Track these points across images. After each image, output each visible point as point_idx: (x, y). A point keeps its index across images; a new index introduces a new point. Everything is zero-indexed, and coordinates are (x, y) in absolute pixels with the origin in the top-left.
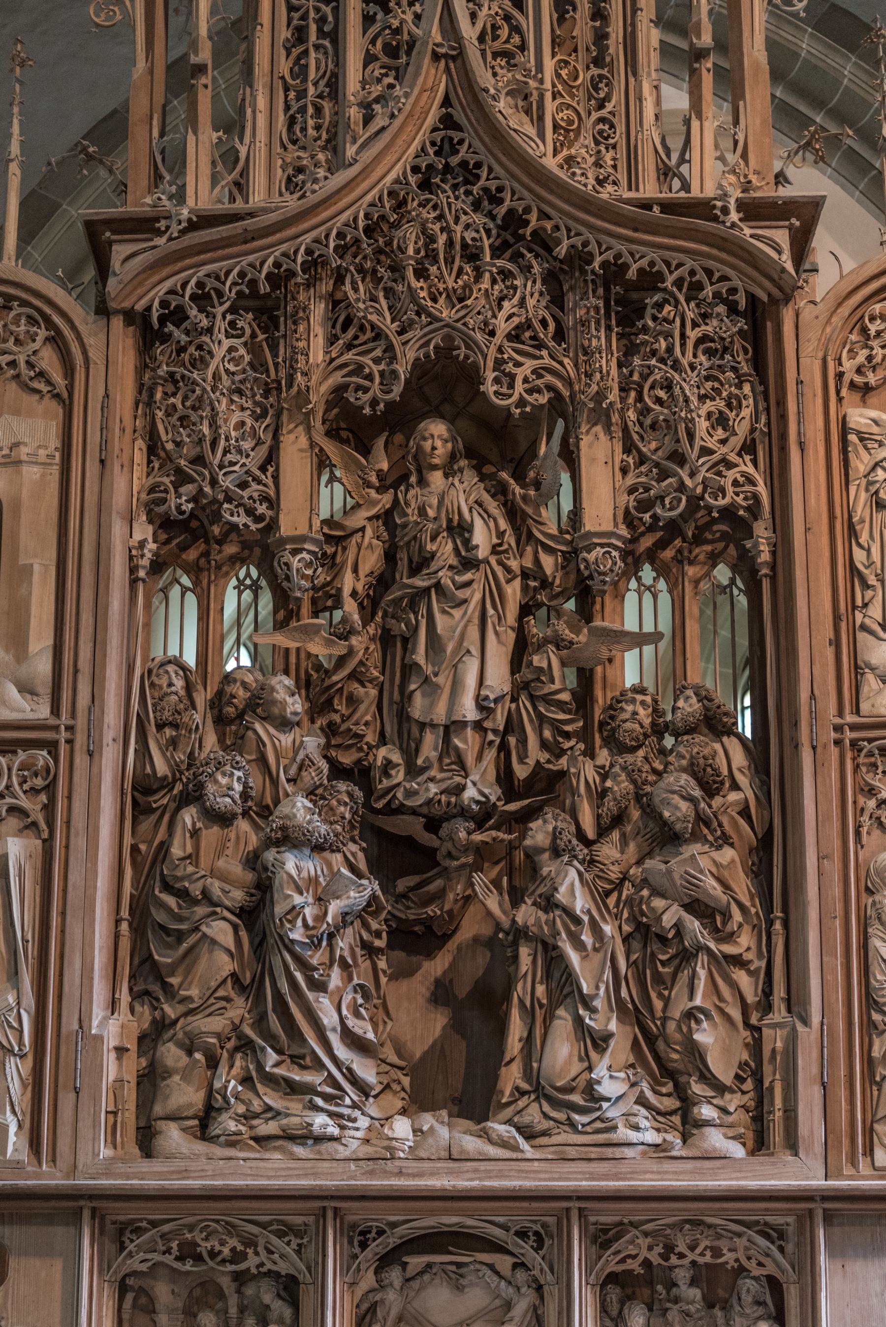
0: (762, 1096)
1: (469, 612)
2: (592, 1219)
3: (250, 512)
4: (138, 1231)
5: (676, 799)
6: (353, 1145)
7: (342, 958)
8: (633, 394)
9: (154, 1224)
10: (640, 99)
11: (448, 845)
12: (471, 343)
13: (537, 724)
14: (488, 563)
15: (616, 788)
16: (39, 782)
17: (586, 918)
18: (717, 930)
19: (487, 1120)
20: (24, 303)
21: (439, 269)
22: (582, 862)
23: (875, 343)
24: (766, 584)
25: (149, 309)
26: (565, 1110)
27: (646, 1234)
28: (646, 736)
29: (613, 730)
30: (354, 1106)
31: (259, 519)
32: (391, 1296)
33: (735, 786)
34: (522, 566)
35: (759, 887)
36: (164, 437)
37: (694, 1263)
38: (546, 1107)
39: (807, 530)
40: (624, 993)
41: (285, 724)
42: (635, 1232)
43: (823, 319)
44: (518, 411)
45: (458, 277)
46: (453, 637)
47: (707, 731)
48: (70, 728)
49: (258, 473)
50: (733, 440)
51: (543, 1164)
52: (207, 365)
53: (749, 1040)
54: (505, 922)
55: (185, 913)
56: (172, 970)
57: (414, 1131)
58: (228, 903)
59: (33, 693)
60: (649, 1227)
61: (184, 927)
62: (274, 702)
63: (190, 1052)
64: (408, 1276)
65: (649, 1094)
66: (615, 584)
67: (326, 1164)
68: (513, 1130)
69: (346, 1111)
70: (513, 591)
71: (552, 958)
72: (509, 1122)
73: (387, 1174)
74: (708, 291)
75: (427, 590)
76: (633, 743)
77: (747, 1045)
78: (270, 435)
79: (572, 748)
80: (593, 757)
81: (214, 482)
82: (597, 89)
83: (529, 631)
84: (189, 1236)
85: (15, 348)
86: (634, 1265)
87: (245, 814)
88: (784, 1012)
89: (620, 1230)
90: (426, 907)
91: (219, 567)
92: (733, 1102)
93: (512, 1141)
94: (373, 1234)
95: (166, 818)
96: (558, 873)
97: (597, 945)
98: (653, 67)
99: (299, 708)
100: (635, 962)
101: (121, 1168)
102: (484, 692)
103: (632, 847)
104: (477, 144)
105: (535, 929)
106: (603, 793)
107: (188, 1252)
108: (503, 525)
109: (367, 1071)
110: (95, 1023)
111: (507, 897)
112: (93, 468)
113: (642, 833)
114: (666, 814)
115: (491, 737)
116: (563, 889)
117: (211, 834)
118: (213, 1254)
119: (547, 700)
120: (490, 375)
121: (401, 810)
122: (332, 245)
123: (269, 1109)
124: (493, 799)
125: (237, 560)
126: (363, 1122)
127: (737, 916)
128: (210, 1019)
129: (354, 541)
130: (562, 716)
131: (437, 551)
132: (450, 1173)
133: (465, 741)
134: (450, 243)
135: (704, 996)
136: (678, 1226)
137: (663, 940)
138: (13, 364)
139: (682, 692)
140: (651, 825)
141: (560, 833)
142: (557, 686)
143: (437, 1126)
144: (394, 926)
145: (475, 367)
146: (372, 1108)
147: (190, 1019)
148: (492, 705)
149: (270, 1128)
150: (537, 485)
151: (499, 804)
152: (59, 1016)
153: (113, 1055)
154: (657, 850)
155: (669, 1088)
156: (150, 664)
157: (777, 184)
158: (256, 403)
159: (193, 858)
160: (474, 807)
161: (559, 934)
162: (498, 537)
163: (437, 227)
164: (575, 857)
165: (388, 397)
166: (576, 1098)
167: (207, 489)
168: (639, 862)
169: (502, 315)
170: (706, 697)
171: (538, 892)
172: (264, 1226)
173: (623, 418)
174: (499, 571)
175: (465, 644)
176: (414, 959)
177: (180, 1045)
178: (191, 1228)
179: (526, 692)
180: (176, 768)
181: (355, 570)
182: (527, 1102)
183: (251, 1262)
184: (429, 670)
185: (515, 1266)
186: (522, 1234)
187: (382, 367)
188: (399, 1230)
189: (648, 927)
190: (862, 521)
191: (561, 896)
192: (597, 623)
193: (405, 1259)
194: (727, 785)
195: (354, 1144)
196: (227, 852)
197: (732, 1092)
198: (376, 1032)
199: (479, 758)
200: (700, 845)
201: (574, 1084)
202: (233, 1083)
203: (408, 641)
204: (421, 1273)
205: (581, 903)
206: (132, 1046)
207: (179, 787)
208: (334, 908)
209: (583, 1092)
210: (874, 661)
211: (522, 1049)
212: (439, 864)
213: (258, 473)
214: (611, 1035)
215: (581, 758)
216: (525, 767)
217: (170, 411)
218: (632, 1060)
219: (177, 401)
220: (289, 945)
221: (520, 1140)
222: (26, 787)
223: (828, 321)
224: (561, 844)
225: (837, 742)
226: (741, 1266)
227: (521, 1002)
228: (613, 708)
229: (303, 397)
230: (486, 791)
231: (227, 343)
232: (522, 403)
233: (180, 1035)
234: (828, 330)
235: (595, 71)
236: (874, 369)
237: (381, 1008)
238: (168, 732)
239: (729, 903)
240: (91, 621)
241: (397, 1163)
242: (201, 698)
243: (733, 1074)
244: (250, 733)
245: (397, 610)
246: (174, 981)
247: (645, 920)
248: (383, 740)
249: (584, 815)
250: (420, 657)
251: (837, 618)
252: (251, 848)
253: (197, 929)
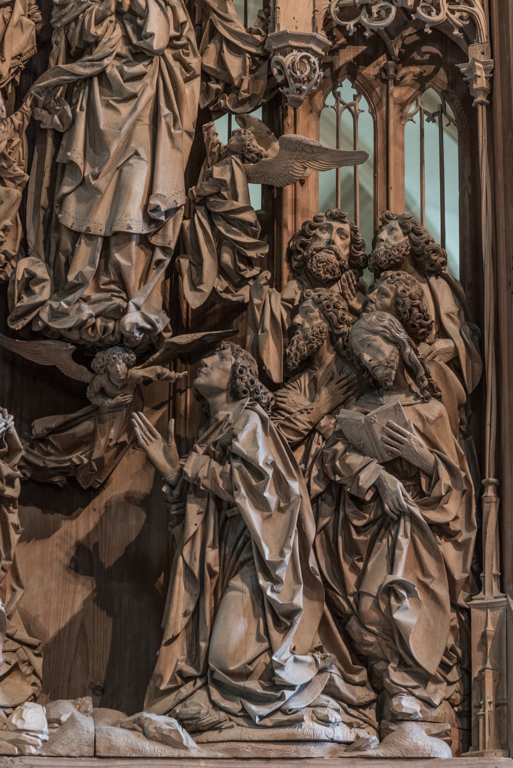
1: (140, 108)
11: (101, 380)
13: (215, 245)
14: (164, 56)
15: (307, 325)
17: (270, 472)
19: (140, 709)
22: (266, 407)
26: (239, 699)
28: (343, 269)
29: (305, 260)
33: (443, 334)
34: (202, 64)
35: (468, 448)
38: (216, 695)
40: (312, 562)
46: (119, 135)
47: (412, 269)
66: (311, 95)
68: (175, 722)
71: (226, 518)
76: (329, 276)
79: (254, 278)
80: (280, 289)
83: (209, 139)
90: (70, 454)
93: (173, 736)
96: (237, 418)
97: (282, 505)
100: (324, 528)
103: (324, 394)
105: (207, 483)
106: (294, 328)
108: (183, 16)
111: (173, 444)
113: (337, 378)
115: (159, 255)
116: (243, 436)
124: (160, 327)
130: (245, 239)
131: (103, 36)
133: (129, 258)
139: (384, 223)
140: (347, 370)
141: (241, 372)
142: (240, 203)
144: (29, 475)
148: (163, 218)
151: (166, 335)
154: (353, 399)
160: (137, 334)
161: (237, 489)
162: (176, 29)
164: (258, 400)
168: (332, 412)
170: (413, 230)
171: (213, 439)
174: (176, 67)
175: (133, 145)
176: (51, 517)
179: (203, 208)
182: (191, 690)
184: (88, 171)
192: (289, 135)
194: (434, 332)
199: (145, 279)
200: (403, 396)
201: (251, 668)
209: (261, 678)
211: (187, 626)
214: (297, 611)
215: (267, 288)
216: (198, 294)
218: (318, 642)
221: (184, 734)
224: (242, 385)
227: (187, 568)
230: (153, 317)
239: (436, 464)
247: (338, 478)
249: (268, 353)
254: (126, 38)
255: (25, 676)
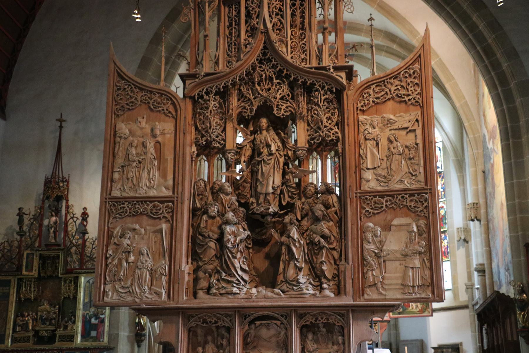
0: (339, 281)
2: (299, 312)
3: (219, 143)
4: (193, 317)
5: (318, 211)
6: (243, 295)
7: (240, 251)
8: (310, 112)
9: (197, 315)
10: (312, 38)
12: (271, 101)
16: (170, 210)
17: (297, 240)
18: (329, 242)
19: (275, 288)
20: (165, 95)
21: (263, 83)
22: (297, 226)
23: (366, 100)
24: (341, 158)
25: (195, 95)
27: (311, 315)
29: (306, 193)
30: (243, 286)
31: (221, 145)
32: (252, 331)
36: (199, 126)
37: (322, 322)
38: (288, 285)
39: (349, 146)
41: (227, 194)
42: (308, 315)
43: (353, 94)
44: (282, 117)
45: (268, 85)
48: (177, 197)
49: (221, 134)
50: (333, 123)
51: (287, 299)
52: (208, 109)
53: (337, 268)
54: (279, 241)
55: (204, 240)
56: (202, 253)
57: (257, 291)
58: (214, 238)
59: (169, 189)
60: (312, 314)
61: (204, 244)
62: (225, 189)
63: (205, 274)
64: (257, 326)
65: (312, 282)
67: (236, 300)
69: (241, 287)
70: (282, 160)
72: (279, 289)
73: (250, 302)
74: (326, 88)
75: (261, 161)
77: (336, 269)
78: (224, 124)
81: (210, 137)
82: (302, 36)
84: (205, 318)
85: (163, 106)
86: (308, 323)
87: (218, 216)
88: (344, 261)
89: (305, 314)
91: (213, 155)
92: (331, 283)
94: (248, 316)
95: (200, 217)
98: (316, 29)
99: (231, 190)
101: (189, 302)
102: (274, 186)
103: (309, 222)
104: (272, 53)
107: (204, 321)
109: (246, 277)
110: (183, 267)
112: (182, 134)
114: (316, 214)
115: (276, 196)
116: (292, 233)
117: (210, 221)
118: (210, 322)
119: (290, 186)
120: (275, 109)
121: (255, 213)
122: (238, 79)
123: (223, 287)
124: (276, 211)
125: (217, 153)
126: (245, 289)
127: (333, 238)
128: (210, 266)
129: (244, 148)
130: (293, 190)
132: (265, 301)
133: (270, 197)
134: (266, 76)
135: (325, 258)
136: (319, 313)
137: (316, 245)
138: (163, 110)
142: (292, 183)
143: (262, 290)
145: (272, 106)
146: (248, 286)
147: (205, 266)
149: (223, 291)
150: (287, 134)
152: (174, 266)
153: (187, 275)
155: (317, 280)
156: (196, 180)
157: (345, 57)
158: (220, 117)
159: (206, 227)
163: (263, 73)
164: (295, 225)
165: (252, 114)
166: (294, 283)
167: (209, 139)
169: (278, 94)
172: (222, 315)
173: (307, 117)
177: (203, 272)
178: (205, 316)
180: (202, 205)
181: (245, 155)
183: (219, 324)
185: (281, 324)
186: (282, 316)
187: (250, 107)
188: (254, 315)
189: (312, 241)
190: (362, 143)
191: (291, 235)
193: (256, 322)
195: (243, 295)
196: (214, 225)
197: (332, 281)
198: (249, 268)
199: (274, 201)
202: (215, 281)
203: (257, 172)
204: (259, 326)
205: (296, 236)
206: (192, 272)
207: (203, 210)
208: (238, 239)
210: (364, 177)
212: (264, 226)
213: (221, 134)
217: (200, 120)
218: (309, 273)
219: (202, 117)
220: (228, 248)
222: (167, 211)
223: (355, 94)
225: (356, 197)
226: (334, 323)
227: (283, 260)
228: (306, 188)
229: (231, 116)
230: (275, 209)
231: (213, 103)
232: (283, 115)
233: (203, 269)
234: (355, 97)
235: (301, 32)
236: (366, 106)
237: (251, 261)
238: (200, 196)
240: (182, 171)
241: (253, 299)
242: (208, 188)
243: (331, 277)
244: (219, 197)
245: (254, 165)
246: (202, 256)
248: (251, 196)
250: (259, 177)
251: (356, 167)
252: (220, 224)
253: (207, 244)
254: (268, 152)
255: (254, 282)
